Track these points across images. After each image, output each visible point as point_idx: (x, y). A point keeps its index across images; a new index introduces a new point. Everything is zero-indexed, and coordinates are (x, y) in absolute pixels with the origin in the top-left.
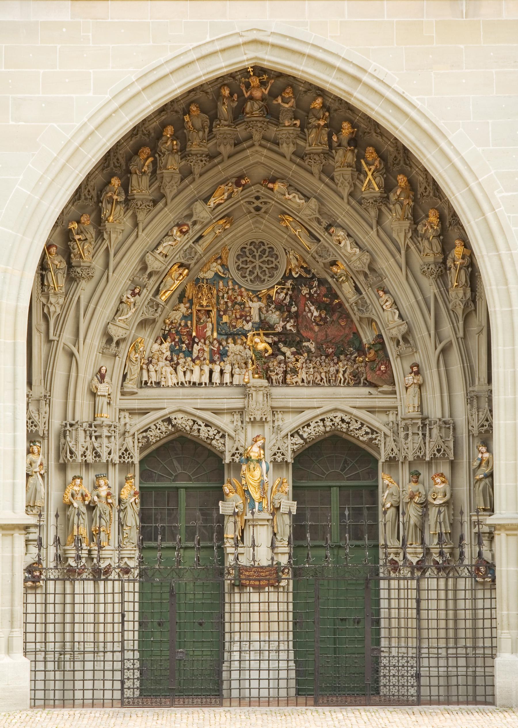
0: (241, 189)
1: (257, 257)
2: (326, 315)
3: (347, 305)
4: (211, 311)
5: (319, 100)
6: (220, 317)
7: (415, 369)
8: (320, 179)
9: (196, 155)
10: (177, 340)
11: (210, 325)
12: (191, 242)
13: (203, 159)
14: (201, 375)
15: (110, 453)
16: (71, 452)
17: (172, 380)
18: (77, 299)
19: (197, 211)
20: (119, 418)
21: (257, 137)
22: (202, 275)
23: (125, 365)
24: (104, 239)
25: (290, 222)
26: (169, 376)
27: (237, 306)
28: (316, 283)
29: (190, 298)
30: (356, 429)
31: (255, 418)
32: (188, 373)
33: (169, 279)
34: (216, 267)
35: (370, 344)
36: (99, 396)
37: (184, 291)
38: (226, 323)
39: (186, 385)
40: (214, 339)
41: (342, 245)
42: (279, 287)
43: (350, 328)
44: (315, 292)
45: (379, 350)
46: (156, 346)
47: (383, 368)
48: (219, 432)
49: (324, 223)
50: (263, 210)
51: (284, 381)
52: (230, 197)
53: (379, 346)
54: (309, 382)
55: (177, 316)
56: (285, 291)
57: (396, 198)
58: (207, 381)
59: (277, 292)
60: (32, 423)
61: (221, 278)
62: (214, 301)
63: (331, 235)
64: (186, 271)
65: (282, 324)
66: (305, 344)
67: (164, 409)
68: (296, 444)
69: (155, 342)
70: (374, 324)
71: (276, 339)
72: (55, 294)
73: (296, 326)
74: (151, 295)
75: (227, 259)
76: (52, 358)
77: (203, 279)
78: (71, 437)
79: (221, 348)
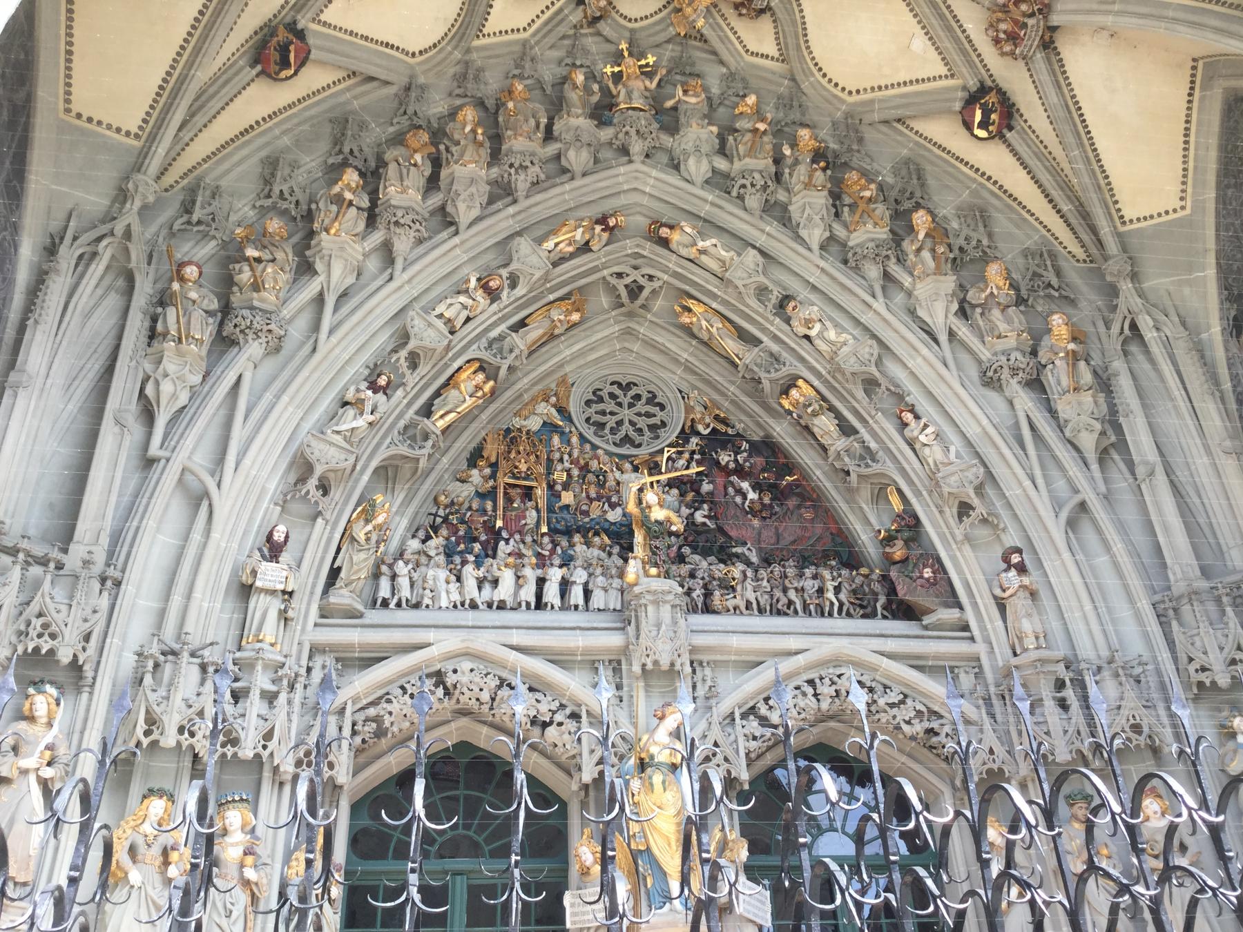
0: (605, 235)
2: (771, 499)
5: (751, 99)
7: (1015, 559)
9: (522, 153)
10: (461, 533)
12: (503, 327)
13: (536, 161)
14: (519, 586)
15: (268, 736)
16: (152, 722)
17: (448, 594)
18: (231, 378)
20: (309, 670)
21: (637, 147)
22: (517, 422)
23: (339, 550)
24: (316, 273)
26: (442, 586)
27: (591, 477)
28: (745, 445)
29: (493, 459)
30: (892, 705)
31: (656, 663)
32: (487, 587)
34: (546, 410)
36: (261, 590)
38: (567, 507)
39: (481, 607)
40: (543, 535)
42: (673, 450)
46: (414, 544)
47: (928, 573)
48: (562, 706)
49: (775, 293)
50: (645, 293)
51: (708, 609)
52: (585, 248)
55: (464, 492)
59: (669, 458)
60: (45, 626)
62: (542, 470)
63: (788, 321)
64: (491, 383)
67: (429, 645)
68: (755, 738)
69: (414, 536)
72: (180, 354)
74: (411, 413)
76: (147, 495)
77: (519, 430)
78: (158, 681)
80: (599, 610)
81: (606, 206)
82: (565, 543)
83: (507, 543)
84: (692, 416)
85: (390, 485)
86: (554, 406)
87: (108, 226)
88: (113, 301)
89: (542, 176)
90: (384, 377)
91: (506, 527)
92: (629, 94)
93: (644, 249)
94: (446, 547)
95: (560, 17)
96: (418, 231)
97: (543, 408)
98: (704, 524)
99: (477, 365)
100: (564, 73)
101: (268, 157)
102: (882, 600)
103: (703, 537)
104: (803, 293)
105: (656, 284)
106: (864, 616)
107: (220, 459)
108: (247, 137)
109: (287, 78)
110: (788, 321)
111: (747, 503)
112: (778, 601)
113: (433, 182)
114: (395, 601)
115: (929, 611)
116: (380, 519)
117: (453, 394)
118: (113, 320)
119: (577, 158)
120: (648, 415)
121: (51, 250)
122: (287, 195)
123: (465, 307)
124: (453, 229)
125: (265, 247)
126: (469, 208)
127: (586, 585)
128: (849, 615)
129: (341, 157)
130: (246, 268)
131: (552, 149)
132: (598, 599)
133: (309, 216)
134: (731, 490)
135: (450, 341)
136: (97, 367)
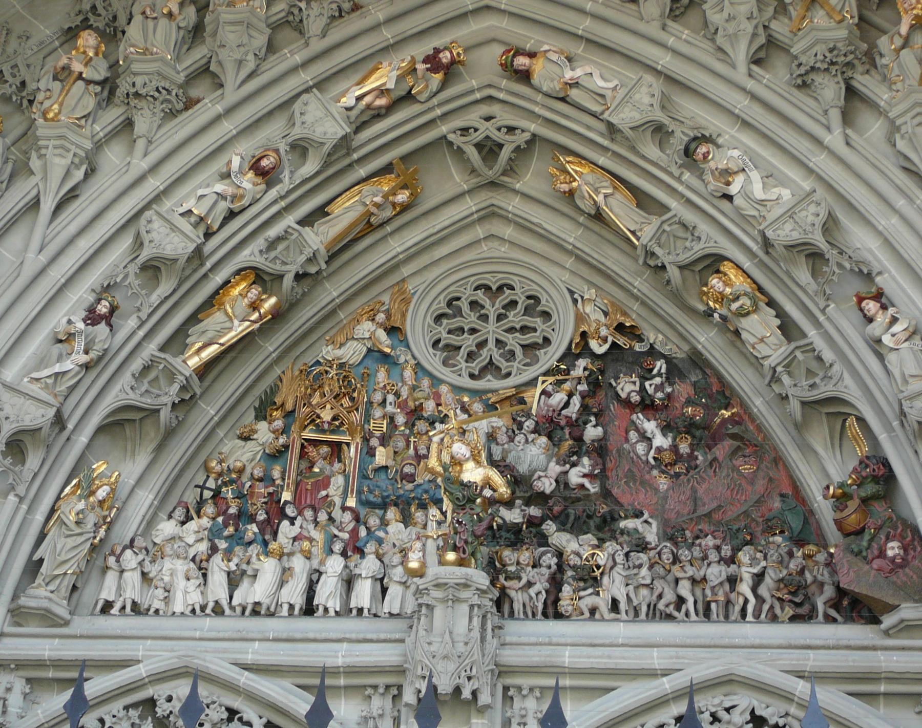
0: (438, 77)
1: (492, 318)
3: (759, 404)
4: (348, 445)
6: (371, 453)
10: (233, 510)
11: (338, 481)
14: (282, 583)
22: (328, 352)
25: (580, 174)
28: (660, 365)
29: (289, 406)
35: (841, 485)
37: (274, 390)
38: (385, 468)
39: (228, 611)
41: (734, 189)
42: (551, 379)
43: (771, 480)
44: (659, 388)
45: (875, 497)
46: (167, 528)
47: (893, 549)
50: (505, 153)
53: (870, 489)
54: (637, 613)
56: (567, 386)
57: (898, 42)
58: (299, 601)
59: (544, 392)
61: (386, 358)
65: (555, 469)
70: (851, 421)
71: (535, 511)
73: (600, 476)
74: (151, 348)
75: (404, 315)
77: (330, 363)
79: (363, 532)
80: (391, 615)
82: (373, 521)
83: (293, 524)
84: (584, 328)
85: (129, 454)
86: (380, 325)
90: (104, 302)
91: (296, 501)
94: (210, 530)
96: (168, 101)
97: (365, 328)
98: (582, 486)
99: (252, 277)
102: (829, 592)
103: (580, 507)
105: (521, 139)
106: (794, 619)
111: (652, 453)
112: (660, 597)
114: (117, 606)
115: (892, 608)
116: (101, 493)
117: (216, 319)
120: (524, 329)
123: (221, 196)
124: (220, 92)
126: (240, 63)
128: (774, 619)
134: (633, 435)
135: (198, 251)
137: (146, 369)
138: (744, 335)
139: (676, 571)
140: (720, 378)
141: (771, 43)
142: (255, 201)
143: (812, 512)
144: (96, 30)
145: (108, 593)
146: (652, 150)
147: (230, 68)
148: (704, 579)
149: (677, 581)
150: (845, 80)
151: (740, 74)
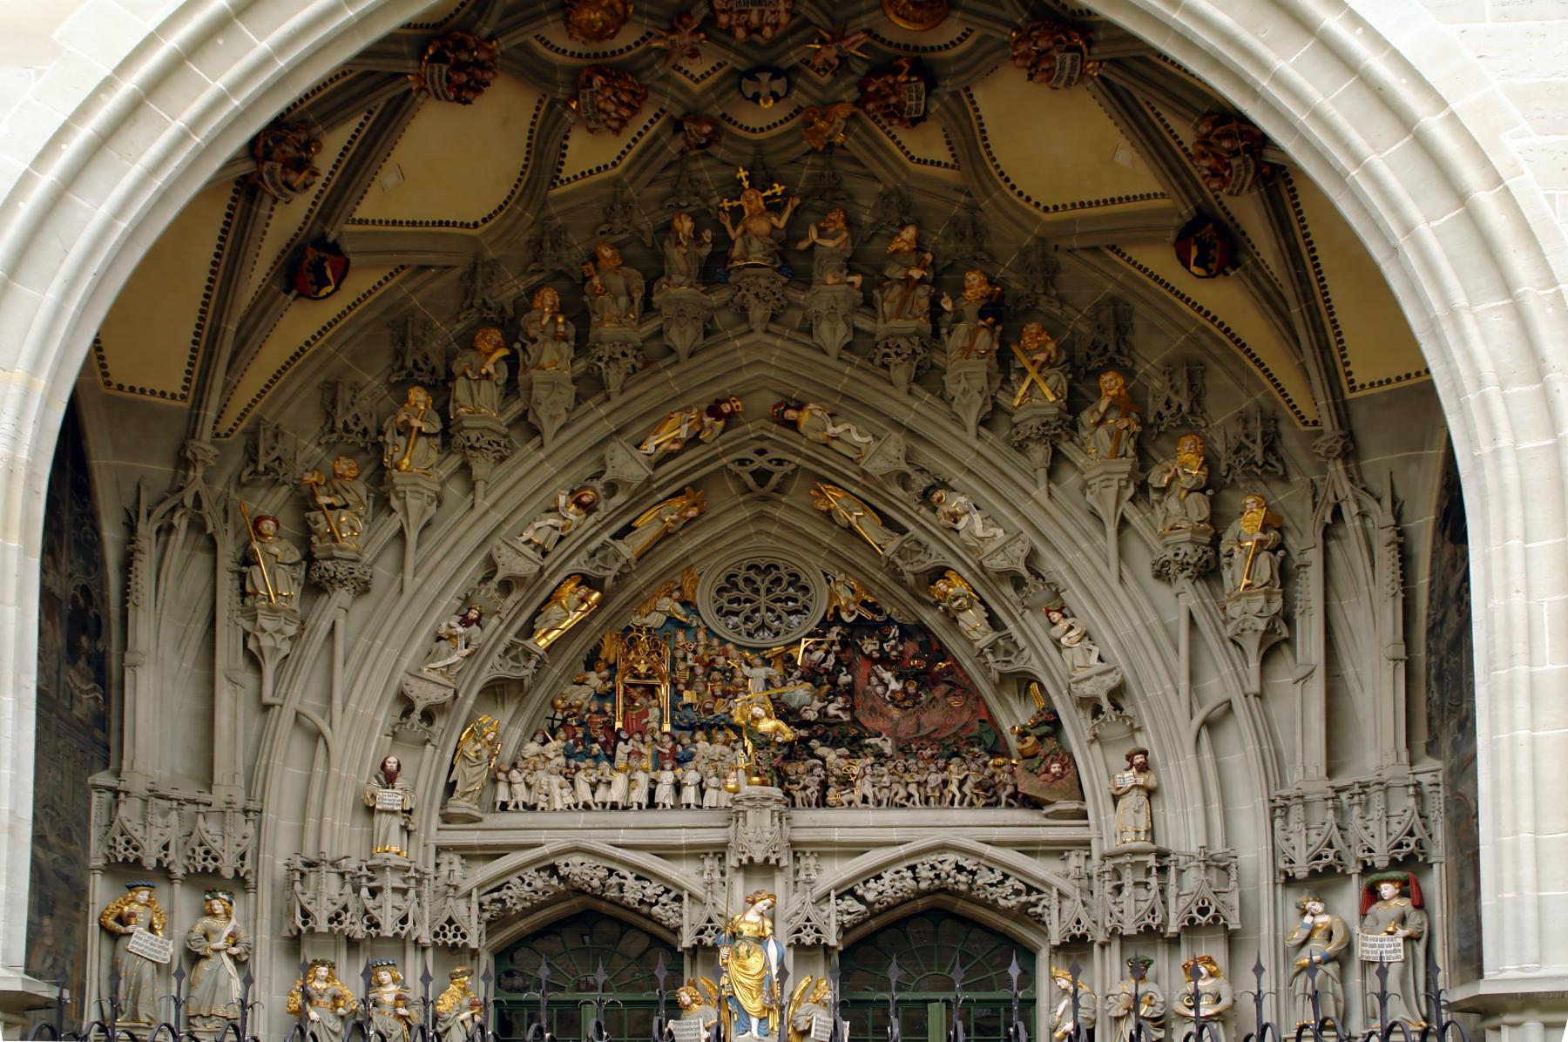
8: (910, 393)
13: (629, 352)
14: (630, 789)
17: (562, 798)
19: (617, 462)
33: (555, 609)
58: (644, 801)
63: (934, 510)
66: (872, 741)
81: (714, 391)
87: (178, 496)
88: (201, 560)
89: (639, 365)
92: (747, 243)
93: (771, 432)
95: (657, 146)
100: (668, 217)
101: (325, 382)
104: (958, 478)
106: (987, 805)
107: (329, 699)
108: (300, 361)
109: (328, 295)
110: (934, 510)
113: (511, 388)
118: (205, 578)
119: (682, 338)
121: (131, 527)
122: (352, 426)
124: (538, 439)
125: (337, 492)
127: (700, 783)
129: (404, 373)
130: (321, 518)
131: (649, 328)
132: (711, 798)
133: (380, 448)
136: (199, 625)
137: (507, 651)
138: (961, 623)
139: (907, 777)
140: (940, 643)
141: (997, 407)
142: (578, 527)
143: (1001, 733)
144: (421, 384)
145: (503, 794)
146: (897, 491)
147: (545, 421)
148: (926, 782)
149: (907, 784)
150: (1052, 446)
151: (970, 437)
